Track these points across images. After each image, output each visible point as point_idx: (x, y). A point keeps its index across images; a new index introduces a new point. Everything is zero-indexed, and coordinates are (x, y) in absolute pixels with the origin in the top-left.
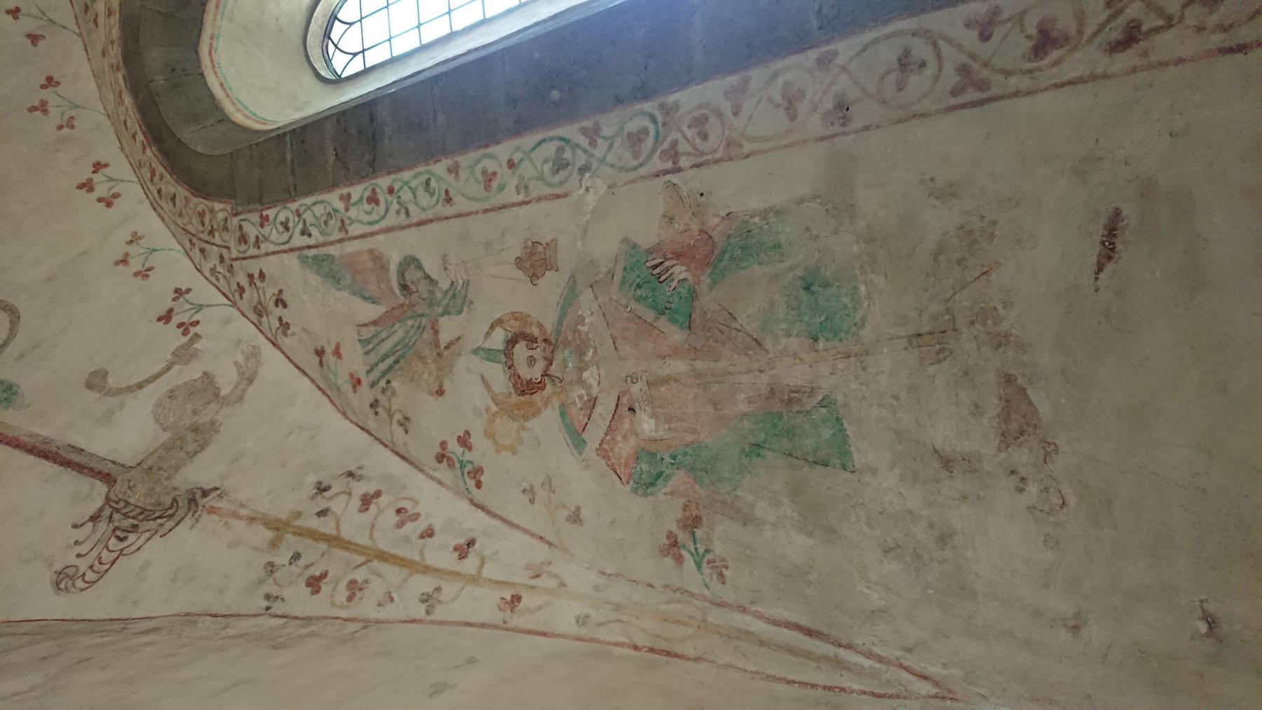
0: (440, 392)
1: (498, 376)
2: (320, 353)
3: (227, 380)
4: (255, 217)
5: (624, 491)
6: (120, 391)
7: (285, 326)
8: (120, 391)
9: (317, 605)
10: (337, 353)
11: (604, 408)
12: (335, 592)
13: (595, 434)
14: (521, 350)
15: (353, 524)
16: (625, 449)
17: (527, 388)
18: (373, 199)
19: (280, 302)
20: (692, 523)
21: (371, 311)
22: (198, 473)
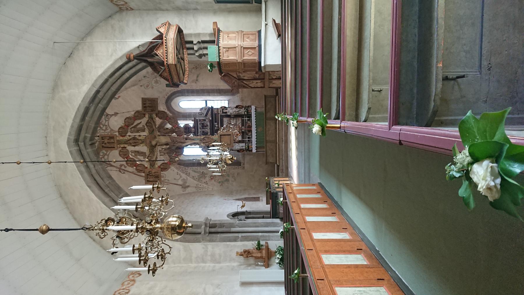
0: (205, 179)
1: (210, 178)
2: (193, 177)
3: (185, 179)
4: (187, 168)
5: (218, 184)
6: (177, 180)
7: (189, 175)
8: (177, 180)
9: (201, 190)
10: (195, 177)
11: (217, 179)
12: (201, 190)
13: (216, 181)
14: (211, 177)
15: (200, 187)
16: (218, 181)
17: (212, 179)
18: (200, 168)
19: (189, 173)
20: (222, 184)
21: (199, 174)
22: (187, 184)
